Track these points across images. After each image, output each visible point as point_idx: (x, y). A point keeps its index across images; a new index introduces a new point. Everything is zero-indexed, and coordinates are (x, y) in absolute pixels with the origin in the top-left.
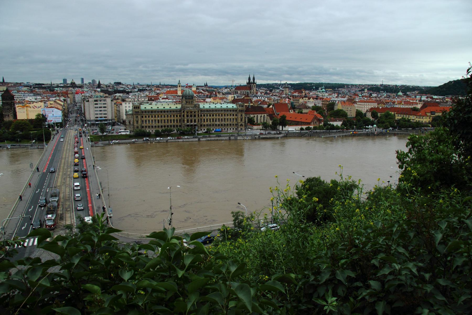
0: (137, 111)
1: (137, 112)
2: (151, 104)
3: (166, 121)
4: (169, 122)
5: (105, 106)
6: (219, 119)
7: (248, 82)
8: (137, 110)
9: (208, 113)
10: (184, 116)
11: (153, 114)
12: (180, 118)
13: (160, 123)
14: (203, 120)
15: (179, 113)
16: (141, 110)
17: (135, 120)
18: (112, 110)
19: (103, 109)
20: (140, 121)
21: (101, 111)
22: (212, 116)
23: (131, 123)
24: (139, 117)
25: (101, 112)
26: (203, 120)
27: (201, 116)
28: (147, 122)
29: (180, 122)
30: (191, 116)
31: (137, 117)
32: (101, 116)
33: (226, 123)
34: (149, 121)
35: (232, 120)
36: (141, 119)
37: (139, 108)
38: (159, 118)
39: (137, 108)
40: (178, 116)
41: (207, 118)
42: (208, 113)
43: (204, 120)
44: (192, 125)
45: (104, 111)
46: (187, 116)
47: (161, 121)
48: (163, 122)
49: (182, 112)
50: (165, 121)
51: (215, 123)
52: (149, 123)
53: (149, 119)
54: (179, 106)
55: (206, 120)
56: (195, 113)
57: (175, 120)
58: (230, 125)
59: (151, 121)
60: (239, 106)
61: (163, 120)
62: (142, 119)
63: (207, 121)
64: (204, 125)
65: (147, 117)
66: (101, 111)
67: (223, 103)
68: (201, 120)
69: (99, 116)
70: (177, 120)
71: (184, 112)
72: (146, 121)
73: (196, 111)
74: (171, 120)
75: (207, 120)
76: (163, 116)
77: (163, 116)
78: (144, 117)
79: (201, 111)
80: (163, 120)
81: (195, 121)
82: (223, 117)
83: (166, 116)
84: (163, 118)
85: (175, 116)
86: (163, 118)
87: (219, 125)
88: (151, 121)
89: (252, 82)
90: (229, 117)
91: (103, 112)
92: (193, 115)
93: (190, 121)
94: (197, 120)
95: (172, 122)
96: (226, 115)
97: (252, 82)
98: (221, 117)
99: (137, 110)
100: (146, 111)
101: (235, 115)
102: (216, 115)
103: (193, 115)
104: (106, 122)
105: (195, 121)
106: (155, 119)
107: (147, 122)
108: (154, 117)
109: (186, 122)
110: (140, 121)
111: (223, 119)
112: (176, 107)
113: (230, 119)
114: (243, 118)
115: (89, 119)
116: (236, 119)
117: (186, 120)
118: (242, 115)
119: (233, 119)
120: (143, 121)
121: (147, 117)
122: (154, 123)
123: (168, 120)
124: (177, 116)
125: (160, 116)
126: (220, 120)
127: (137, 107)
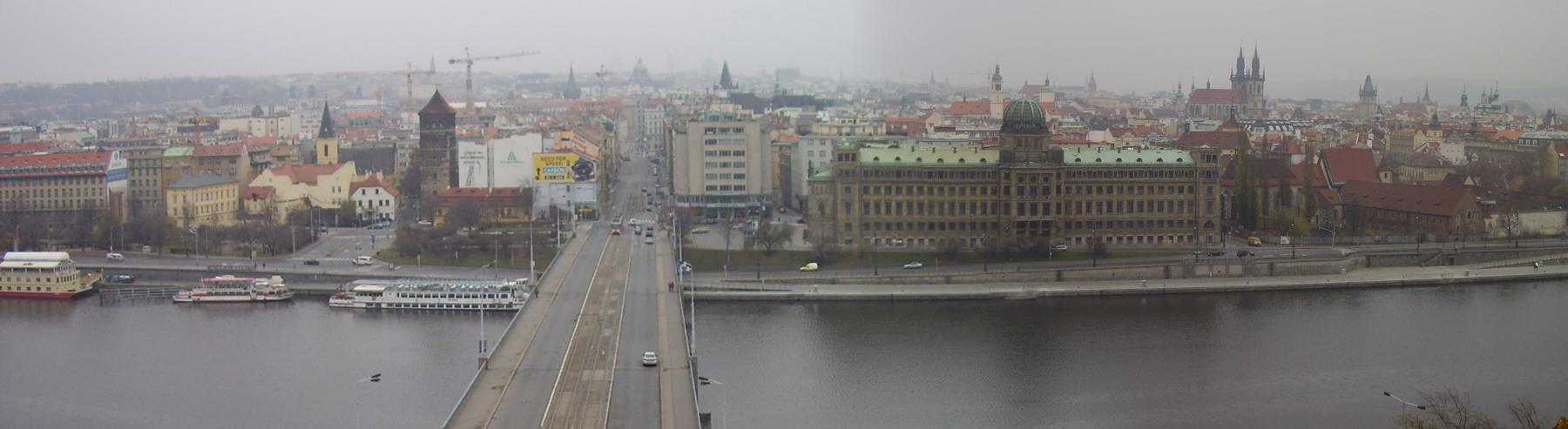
0: (845, 168)
1: (847, 173)
2: (897, 147)
3: (946, 206)
4: (957, 210)
5: (740, 148)
6: (1130, 203)
7: (1235, 73)
8: (847, 165)
9: (1092, 179)
11: (902, 179)
12: (994, 198)
13: (926, 213)
14: (1074, 206)
15: (991, 180)
16: (861, 167)
17: (839, 201)
18: (763, 165)
19: (731, 159)
20: (856, 207)
21: (725, 165)
22: (1105, 191)
23: (828, 210)
24: (855, 189)
25: (725, 171)
26: (1074, 206)
27: (1068, 189)
28: (883, 209)
29: (994, 212)
30: (1033, 190)
31: (848, 189)
32: (724, 182)
33: (1156, 216)
34: (888, 206)
35: (1176, 207)
36: (860, 197)
37: (854, 157)
38: (922, 197)
39: (847, 159)
40: (989, 192)
41: (1089, 198)
42: (1092, 179)
43: (1079, 205)
44: (1034, 224)
45: (739, 165)
46: (1021, 191)
47: (931, 205)
48: (936, 210)
49: (1003, 175)
50: (941, 206)
51: (1116, 216)
52: (888, 211)
53: (888, 197)
54: (992, 157)
55: (1084, 205)
56: (1046, 180)
57: (978, 205)
58: (1171, 223)
59: (894, 204)
60: (1203, 158)
61: (936, 204)
62: (865, 197)
63: (1089, 210)
64: (1079, 225)
65: (883, 190)
66: (725, 165)
67: (1147, 148)
68: (1068, 205)
69: (719, 183)
70: (984, 206)
71: (1007, 176)
72: (877, 206)
73: (1051, 174)
74: (963, 206)
75: (1089, 205)
76: (936, 190)
77: (936, 190)
78: (872, 190)
79: (1069, 174)
80: (936, 204)
81: (1047, 210)
82: (1145, 197)
83: (946, 189)
84: (936, 197)
85: (978, 191)
86: (936, 197)
87: (1130, 224)
88: (894, 204)
89: (1248, 76)
90: (1166, 196)
91: (733, 171)
92: (1040, 190)
93: (1028, 210)
94: (1053, 207)
95: (968, 211)
96: (1156, 190)
97: (1248, 76)
98: (1136, 198)
99: (847, 165)
100: (878, 171)
101: (1186, 191)
102: (1121, 190)
103: (1040, 190)
104: (742, 205)
105: (1047, 210)
106: (908, 198)
107: (883, 209)
108: (904, 191)
109: (1014, 212)
110: (856, 207)
111: (1146, 205)
112: (983, 160)
113: (1171, 204)
114: (1214, 200)
115: (686, 193)
116: (1191, 204)
117: (1014, 204)
118: (1210, 189)
119: (1181, 204)
120: (867, 206)
121: (883, 190)
122: (905, 213)
123: (952, 205)
124: (984, 191)
125: (926, 189)
126: (1135, 205)
127: (847, 155)
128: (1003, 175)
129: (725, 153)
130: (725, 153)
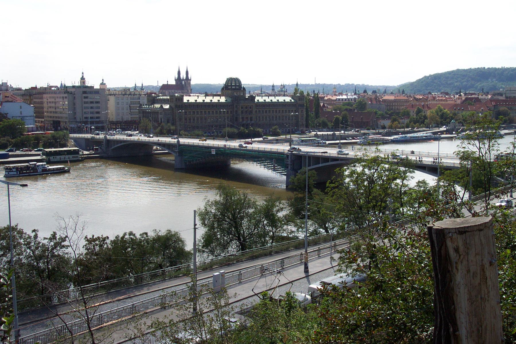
10: (236, 111)
21: (92, 108)
25: (92, 110)
46: (242, 112)
49: (235, 106)
66: (92, 108)
75: (263, 118)
76: (211, 112)
81: (251, 120)
128: (235, 106)
129: (91, 102)
130: (91, 102)
